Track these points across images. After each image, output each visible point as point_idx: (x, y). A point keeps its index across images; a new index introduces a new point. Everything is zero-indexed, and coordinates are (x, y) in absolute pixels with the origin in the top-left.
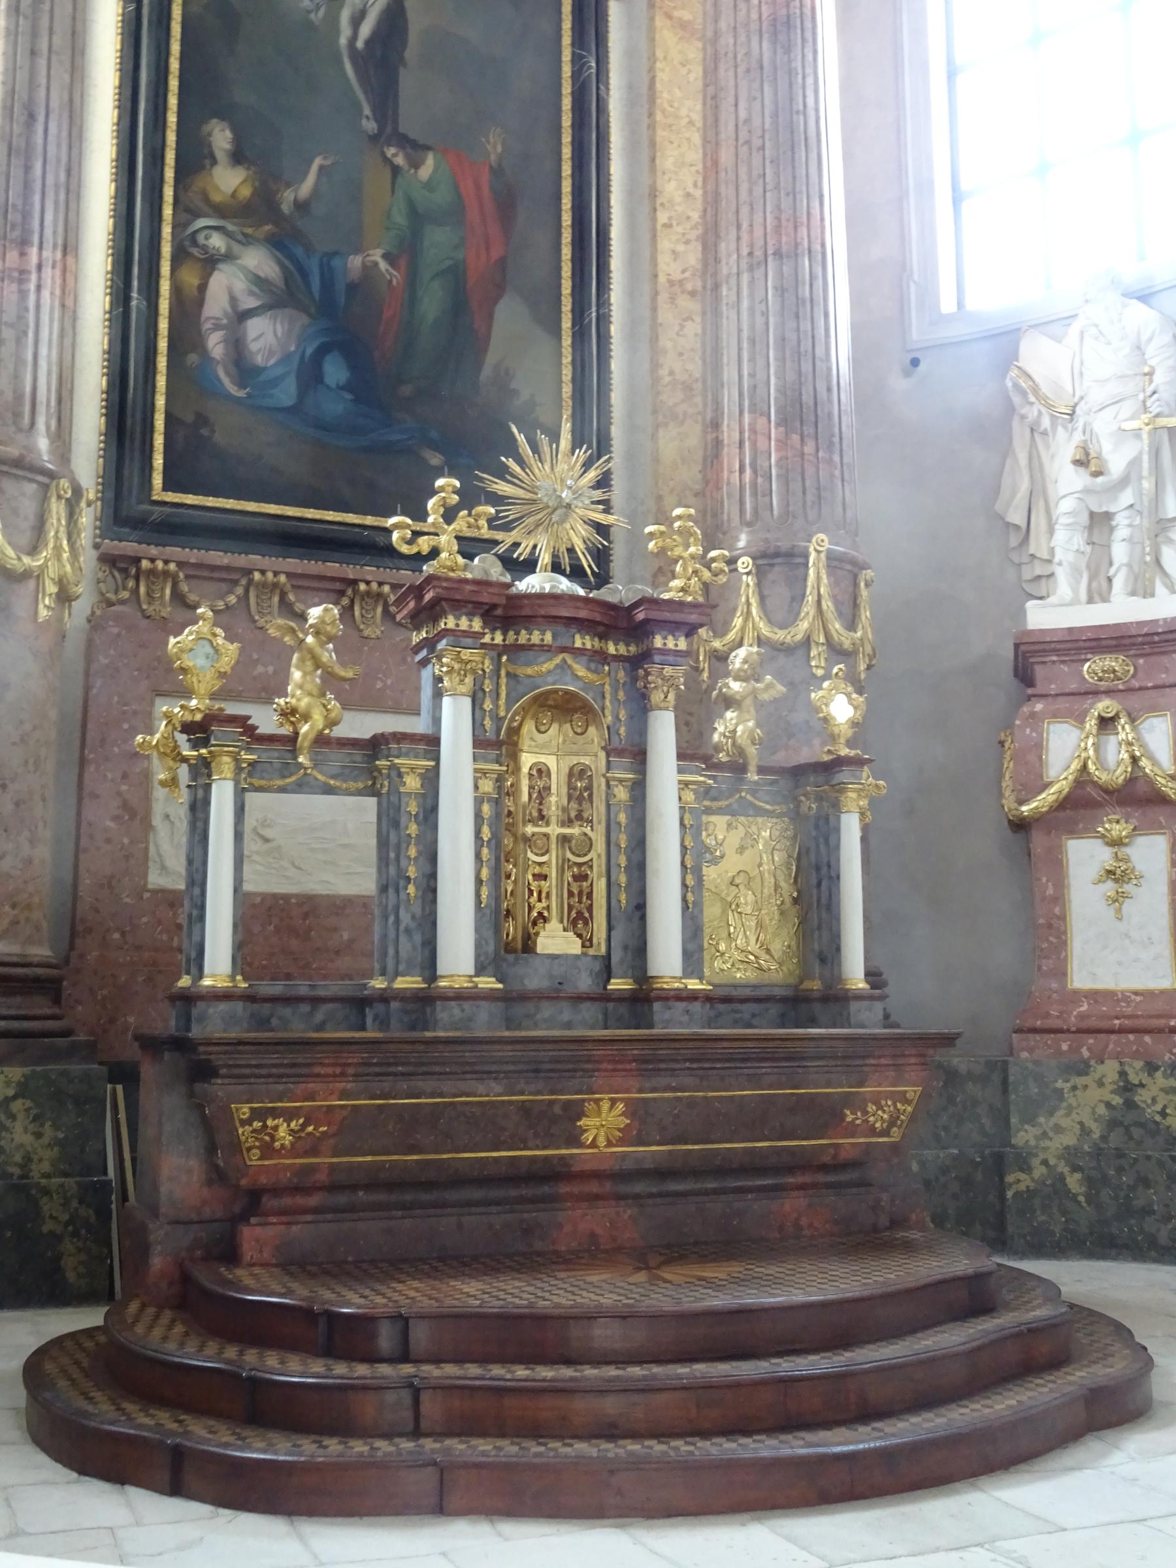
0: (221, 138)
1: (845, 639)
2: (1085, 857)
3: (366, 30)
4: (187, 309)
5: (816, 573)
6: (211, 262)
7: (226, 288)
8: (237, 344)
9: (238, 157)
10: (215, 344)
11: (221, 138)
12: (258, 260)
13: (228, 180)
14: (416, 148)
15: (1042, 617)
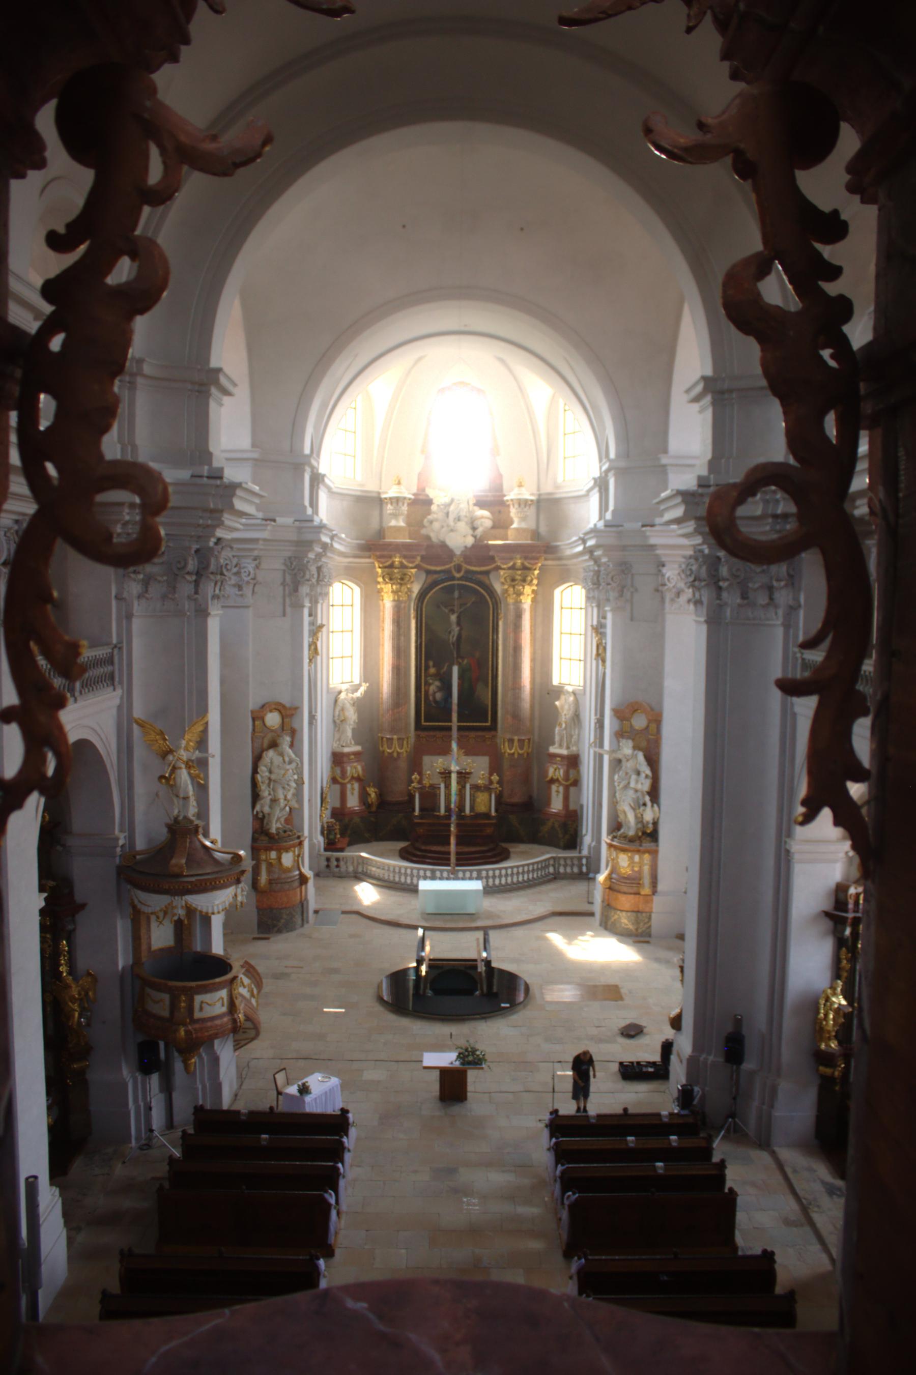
0: (431, 663)
1: (521, 752)
2: (554, 787)
3: (455, 638)
4: (427, 692)
5: (516, 743)
6: (430, 684)
7: (432, 689)
8: (434, 698)
9: (434, 666)
10: (431, 698)
11: (431, 663)
12: (437, 683)
13: (432, 670)
14: (463, 658)
15: (553, 750)
